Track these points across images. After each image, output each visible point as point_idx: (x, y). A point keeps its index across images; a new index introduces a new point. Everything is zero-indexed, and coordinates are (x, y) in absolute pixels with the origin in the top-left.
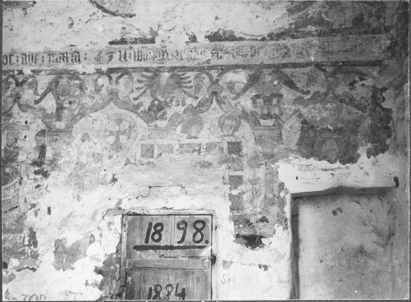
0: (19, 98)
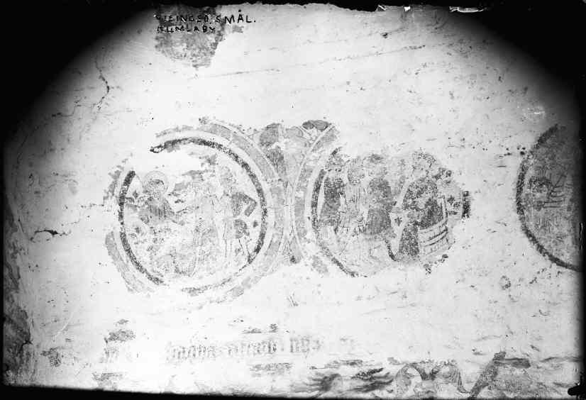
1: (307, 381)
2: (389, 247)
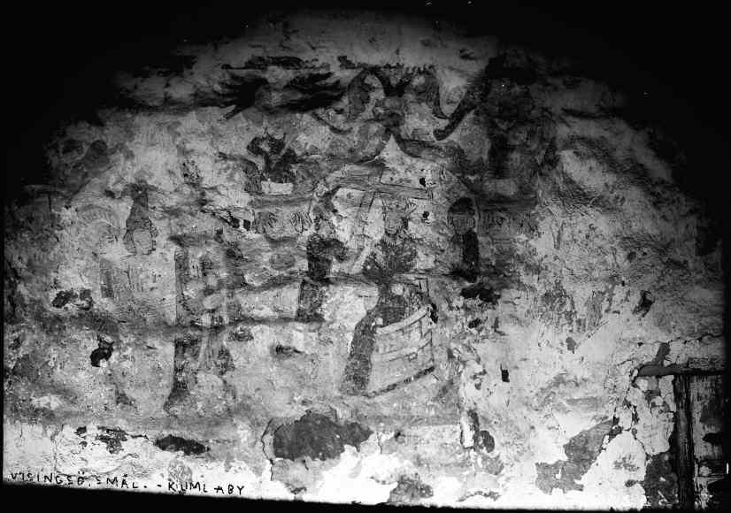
0: (397, 124)
1: (218, 88)
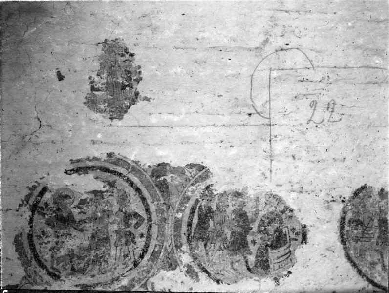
2: (247, 262)
